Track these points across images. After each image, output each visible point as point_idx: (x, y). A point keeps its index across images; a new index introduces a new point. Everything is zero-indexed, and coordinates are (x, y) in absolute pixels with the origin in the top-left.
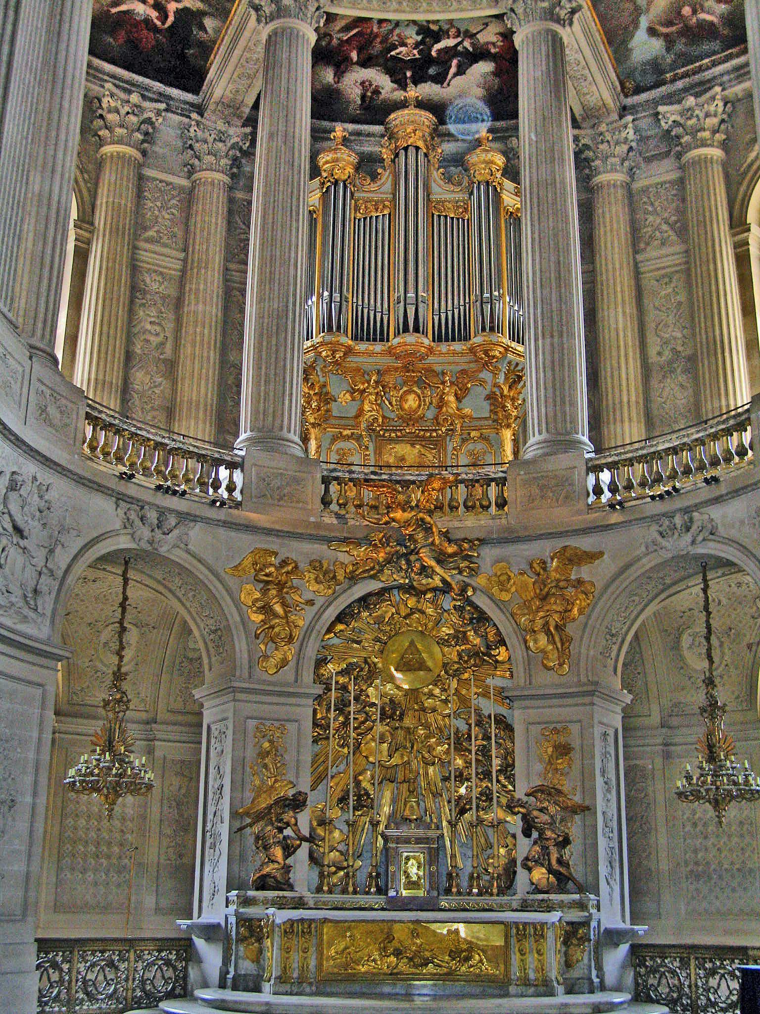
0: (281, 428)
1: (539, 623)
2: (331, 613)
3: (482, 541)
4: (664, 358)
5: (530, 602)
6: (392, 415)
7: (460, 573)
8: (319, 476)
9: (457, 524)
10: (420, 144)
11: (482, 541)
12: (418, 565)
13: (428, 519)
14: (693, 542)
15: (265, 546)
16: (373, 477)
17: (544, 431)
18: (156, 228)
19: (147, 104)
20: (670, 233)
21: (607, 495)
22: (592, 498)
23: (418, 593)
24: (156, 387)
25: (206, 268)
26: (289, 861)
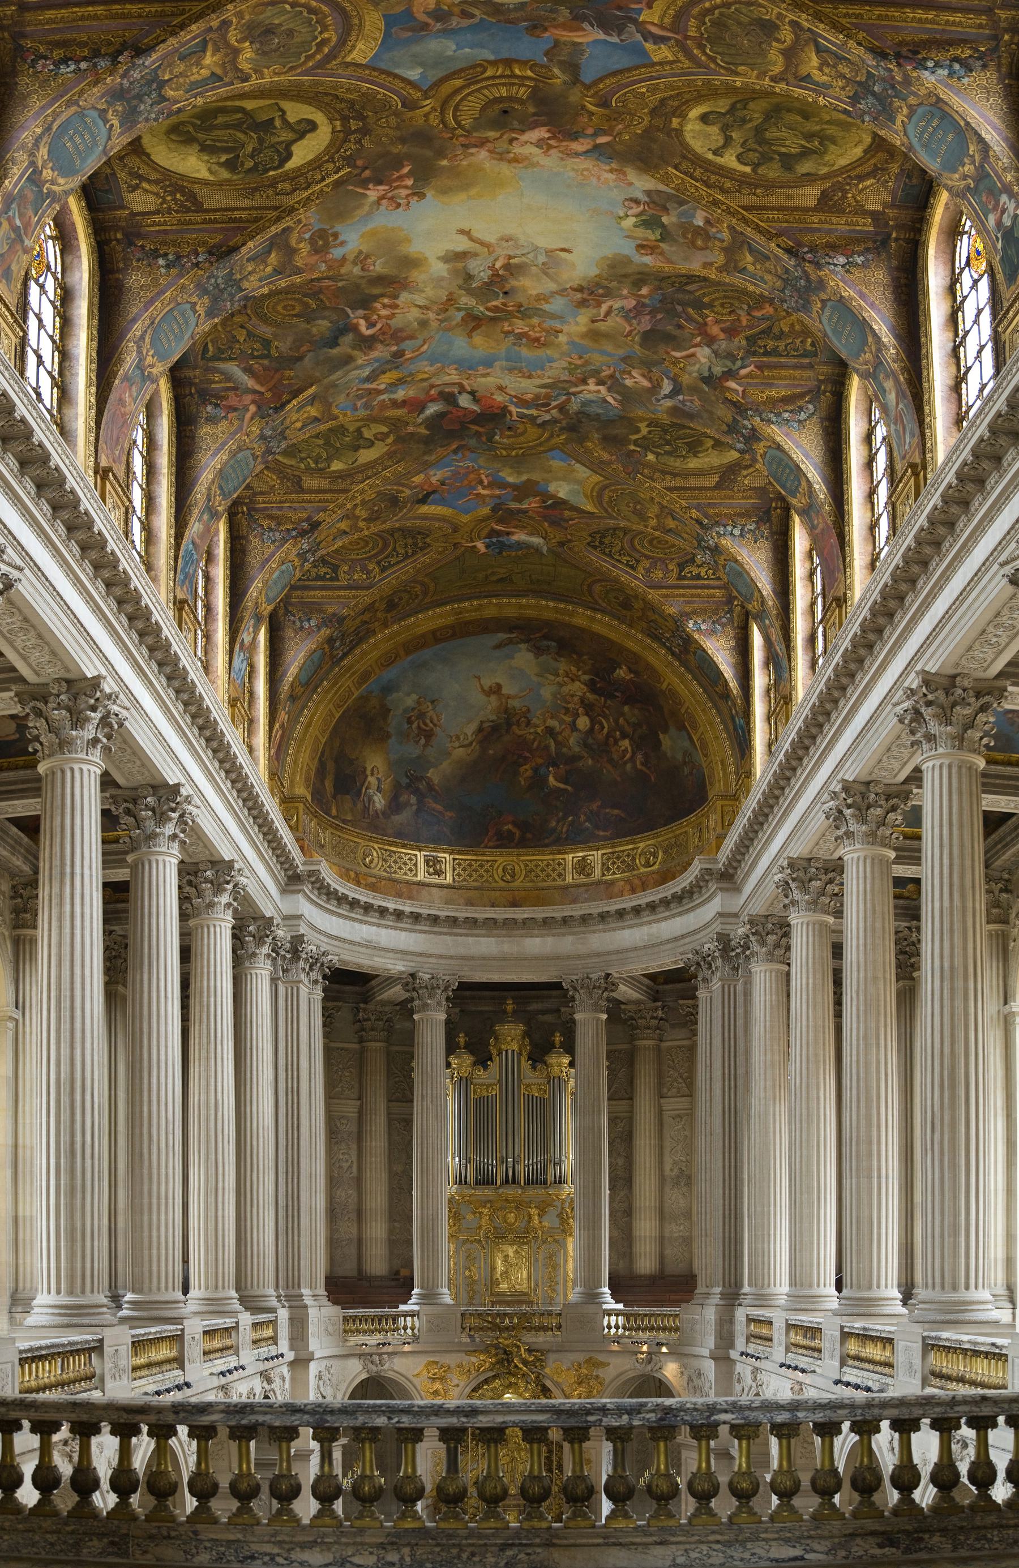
2: (468, 1390)
23: (514, 1375)
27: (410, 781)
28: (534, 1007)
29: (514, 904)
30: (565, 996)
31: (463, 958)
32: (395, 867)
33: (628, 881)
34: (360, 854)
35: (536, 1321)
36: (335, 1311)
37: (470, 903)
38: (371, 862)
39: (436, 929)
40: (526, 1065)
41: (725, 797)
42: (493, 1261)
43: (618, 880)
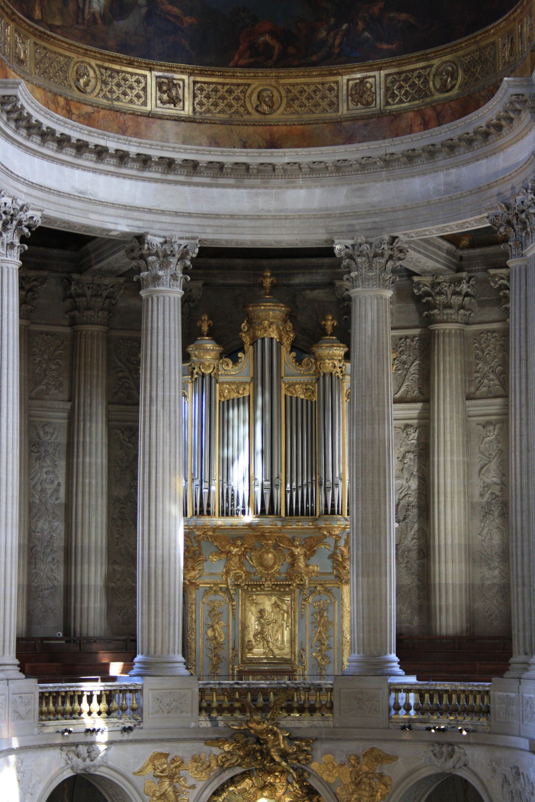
2: (208, 793)
3: (316, 739)
4: (485, 500)
5: (348, 786)
6: (253, 570)
7: (299, 762)
8: (197, 690)
9: (297, 724)
10: (275, 335)
11: (316, 739)
12: (269, 758)
13: (275, 728)
14: (454, 767)
15: (159, 750)
16: (236, 686)
17: (362, 651)
18: (44, 383)
19: (32, 274)
20: (497, 382)
21: (402, 712)
22: (393, 712)
23: (270, 772)
24: (54, 531)
25: (91, 421)
28: (298, 280)
29: (273, 143)
30: (339, 266)
31: (205, 216)
32: (118, 92)
33: (419, 112)
34: (72, 74)
35: (300, 698)
36: (32, 687)
37: (215, 142)
38: (87, 84)
39: (170, 177)
40: (287, 357)
43: (406, 110)
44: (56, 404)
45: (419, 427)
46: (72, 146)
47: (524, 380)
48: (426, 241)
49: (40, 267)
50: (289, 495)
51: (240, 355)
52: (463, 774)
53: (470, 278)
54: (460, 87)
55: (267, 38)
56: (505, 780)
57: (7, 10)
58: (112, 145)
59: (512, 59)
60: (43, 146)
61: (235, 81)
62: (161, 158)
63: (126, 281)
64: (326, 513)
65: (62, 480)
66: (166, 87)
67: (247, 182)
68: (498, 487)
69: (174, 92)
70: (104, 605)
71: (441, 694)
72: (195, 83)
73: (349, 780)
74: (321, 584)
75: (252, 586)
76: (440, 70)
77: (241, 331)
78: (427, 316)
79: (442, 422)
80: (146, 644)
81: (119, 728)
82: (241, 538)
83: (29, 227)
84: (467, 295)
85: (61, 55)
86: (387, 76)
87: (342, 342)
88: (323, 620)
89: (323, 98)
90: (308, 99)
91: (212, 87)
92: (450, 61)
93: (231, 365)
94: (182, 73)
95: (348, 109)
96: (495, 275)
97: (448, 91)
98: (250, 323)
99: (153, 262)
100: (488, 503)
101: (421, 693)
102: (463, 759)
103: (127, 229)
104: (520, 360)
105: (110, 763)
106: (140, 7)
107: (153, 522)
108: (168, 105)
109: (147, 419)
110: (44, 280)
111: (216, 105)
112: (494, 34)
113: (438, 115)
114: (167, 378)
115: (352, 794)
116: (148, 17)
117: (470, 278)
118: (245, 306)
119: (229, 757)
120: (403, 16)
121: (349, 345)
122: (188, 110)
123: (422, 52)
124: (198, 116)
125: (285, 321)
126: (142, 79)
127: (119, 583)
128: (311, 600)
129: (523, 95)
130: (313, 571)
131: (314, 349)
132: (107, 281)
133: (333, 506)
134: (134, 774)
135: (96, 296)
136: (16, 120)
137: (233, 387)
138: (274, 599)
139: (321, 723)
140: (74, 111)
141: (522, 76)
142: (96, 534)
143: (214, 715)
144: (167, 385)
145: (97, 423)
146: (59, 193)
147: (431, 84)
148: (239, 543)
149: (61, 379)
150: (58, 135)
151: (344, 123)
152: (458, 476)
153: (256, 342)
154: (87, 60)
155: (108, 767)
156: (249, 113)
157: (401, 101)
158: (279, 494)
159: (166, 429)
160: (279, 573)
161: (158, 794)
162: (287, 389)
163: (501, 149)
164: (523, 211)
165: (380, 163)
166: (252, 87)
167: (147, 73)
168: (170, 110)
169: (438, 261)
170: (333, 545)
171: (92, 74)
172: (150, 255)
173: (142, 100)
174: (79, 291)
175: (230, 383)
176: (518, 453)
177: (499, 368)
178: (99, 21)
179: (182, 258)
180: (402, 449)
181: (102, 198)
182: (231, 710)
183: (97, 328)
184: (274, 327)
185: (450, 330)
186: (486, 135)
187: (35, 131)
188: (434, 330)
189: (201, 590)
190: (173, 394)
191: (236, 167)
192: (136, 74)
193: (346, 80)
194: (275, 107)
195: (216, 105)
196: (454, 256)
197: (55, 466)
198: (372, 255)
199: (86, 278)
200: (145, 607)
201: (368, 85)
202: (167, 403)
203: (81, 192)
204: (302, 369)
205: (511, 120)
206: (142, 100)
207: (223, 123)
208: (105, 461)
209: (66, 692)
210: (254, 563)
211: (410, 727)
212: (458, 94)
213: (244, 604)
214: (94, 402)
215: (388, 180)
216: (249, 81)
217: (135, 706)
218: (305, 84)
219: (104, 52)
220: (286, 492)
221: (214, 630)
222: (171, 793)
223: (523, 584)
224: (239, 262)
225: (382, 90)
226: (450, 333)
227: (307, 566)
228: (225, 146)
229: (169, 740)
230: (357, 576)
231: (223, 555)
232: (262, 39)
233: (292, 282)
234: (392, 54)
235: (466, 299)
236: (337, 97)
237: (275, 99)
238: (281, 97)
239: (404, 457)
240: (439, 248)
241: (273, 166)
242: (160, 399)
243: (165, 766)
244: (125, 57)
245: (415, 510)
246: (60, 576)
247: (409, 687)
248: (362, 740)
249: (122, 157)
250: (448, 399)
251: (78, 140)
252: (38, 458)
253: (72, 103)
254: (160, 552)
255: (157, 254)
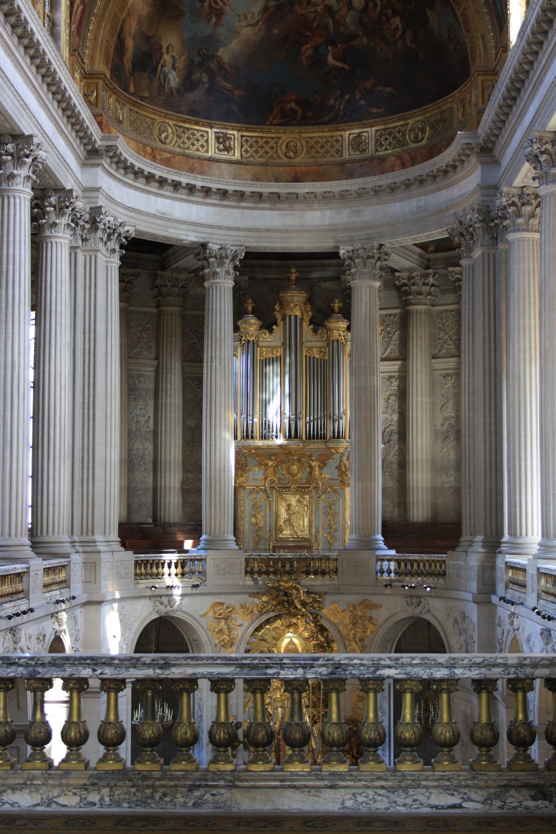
0: (224, 533)
1: (351, 637)
2: (252, 629)
3: (326, 593)
4: (444, 428)
6: (283, 477)
7: (314, 609)
8: (243, 560)
9: (313, 583)
10: (298, 314)
11: (326, 593)
14: (421, 613)
15: (218, 600)
18: (139, 346)
19: (130, 271)
20: (453, 346)
21: (386, 574)
22: (379, 574)
23: (294, 616)
24: (146, 449)
25: (171, 373)
26: (235, 752)
27: (201, 58)
28: (315, 275)
29: (296, 179)
30: (343, 266)
32: (188, 143)
33: (399, 156)
34: (156, 131)
36: (130, 556)
37: (256, 178)
38: (166, 138)
39: (225, 203)
41: (485, 72)
42: (277, 510)
43: (389, 155)
44: (147, 362)
45: (399, 377)
46: (156, 181)
47: (471, 345)
48: (404, 247)
49: (135, 266)
50: (308, 425)
51: (274, 327)
52: (427, 617)
53: (435, 274)
54: (428, 139)
55: (293, 105)
56: (456, 621)
57: (111, 86)
58: (184, 180)
59: (464, 119)
60: (136, 181)
61: (270, 135)
62: (218, 189)
63: (195, 276)
64: (334, 437)
65: (151, 414)
66: (222, 139)
67: (279, 206)
68: (454, 420)
69: (227, 143)
70: (180, 500)
71: (412, 562)
72: (242, 136)
73: (349, 621)
74: (330, 487)
75: (283, 488)
76: (414, 126)
77: (274, 310)
78: (405, 300)
79: (415, 374)
80: (208, 528)
81: (190, 585)
82: (275, 454)
83: (126, 238)
84: (433, 285)
85: (148, 117)
86: (377, 131)
87: (345, 318)
88: (332, 512)
89: (332, 147)
90: (321, 148)
91: (254, 139)
92: (420, 121)
93: (268, 335)
94: (233, 129)
95: (349, 155)
96: (452, 272)
97: (419, 142)
98: (281, 305)
99: (213, 262)
100: (447, 431)
101: (398, 562)
102: (427, 607)
103: (194, 239)
104: (469, 330)
105: (184, 609)
106: (204, 83)
107: (213, 443)
108: (223, 152)
109: (209, 372)
110: (138, 276)
111: (256, 152)
112: (451, 101)
113: (412, 158)
114: (223, 343)
115: (351, 631)
116: (209, 90)
117: (435, 274)
118: (278, 293)
119: (266, 605)
120: (388, 89)
121: (350, 321)
122: (237, 156)
123: (401, 114)
124: (244, 160)
125: (305, 304)
126: (205, 134)
127: (190, 486)
128: (323, 497)
129: (471, 144)
130: (325, 478)
131: (326, 323)
132: (182, 276)
133: (339, 432)
134: (201, 616)
135: (174, 286)
136: (117, 163)
137: (270, 350)
138: (298, 497)
139: (329, 582)
140: (157, 156)
141: (470, 131)
142: (175, 452)
143: (256, 576)
144: (223, 349)
145: (175, 375)
146: (147, 214)
147: (407, 137)
148: (273, 458)
149: (150, 344)
150: (146, 173)
151: (347, 165)
152: (426, 411)
153: (285, 318)
154: (167, 121)
155: (182, 612)
156: (280, 158)
157: (386, 149)
158: (301, 424)
159: (222, 379)
160: (301, 479)
161: (217, 630)
162: (307, 351)
163: (456, 182)
164: (471, 226)
165: (372, 193)
166: (282, 139)
167: (209, 130)
168: (225, 156)
169: (412, 262)
170: (338, 460)
171: (170, 130)
172: (211, 257)
173: (205, 149)
174: (162, 283)
175: (267, 347)
176: (467, 396)
177: (455, 337)
178: (175, 94)
179: (233, 259)
180: (387, 393)
181: (175, 217)
182: (267, 573)
183: (176, 309)
184: (298, 308)
185: (421, 310)
186: (446, 172)
187: (130, 170)
188: (410, 310)
189: (247, 491)
190: (227, 354)
191: (271, 195)
192: (201, 131)
193: (348, 134)
194: (298, 154)
195: (256, 152)
196: (424, 258)
197: (147, 405)
198: (365, 257)
199: (167, 274)
200: (208, 502)
201: (363, 138)
202: (223, 361)
203: (162, 214)
204: (318, 337)
205: (463, 162)
206: (205, 149)
207: (262, 164)
208: (181, 401)
209: (153, 560)
210: (284, 472)
211: (390, 585)
212: (426, 144)
213: (277, 500)
214: (173, 360)
215: (378, 204)
216: (280, 135)
217: (201, 570)
218: (319, 137)
219: (178, 115)
220: (306, 423)
221: (256, 518)
222: (226, 629)
223: (470, 487)
224: (274, 262)
225: (373, 142)
226: (421, 312)
227: (321, 474)
228: (263, 181)
229: (224, 594)
230: (355, 481)
231: (263, 467)
232: (289, 106)
233: (311, 276)
234: (380, 116)
235: (432, 288)
236: (342, 146)
237: (298, 147)
238: (302, 146)
239: (388, 399)
240: (413, 252)
241: (297, 195)
242: (218, 358)
243: (222, 611)
244: (194, 118)
245: (396, 436)
246: (150, 480)
247: (390, 558)
248: (357, 594)
249: (191, 189)
250: (419, 358)
251: (160, 177)
252: (135, 399)
253: (156, 151)
254: (218, 464)
255: (215, 257)
